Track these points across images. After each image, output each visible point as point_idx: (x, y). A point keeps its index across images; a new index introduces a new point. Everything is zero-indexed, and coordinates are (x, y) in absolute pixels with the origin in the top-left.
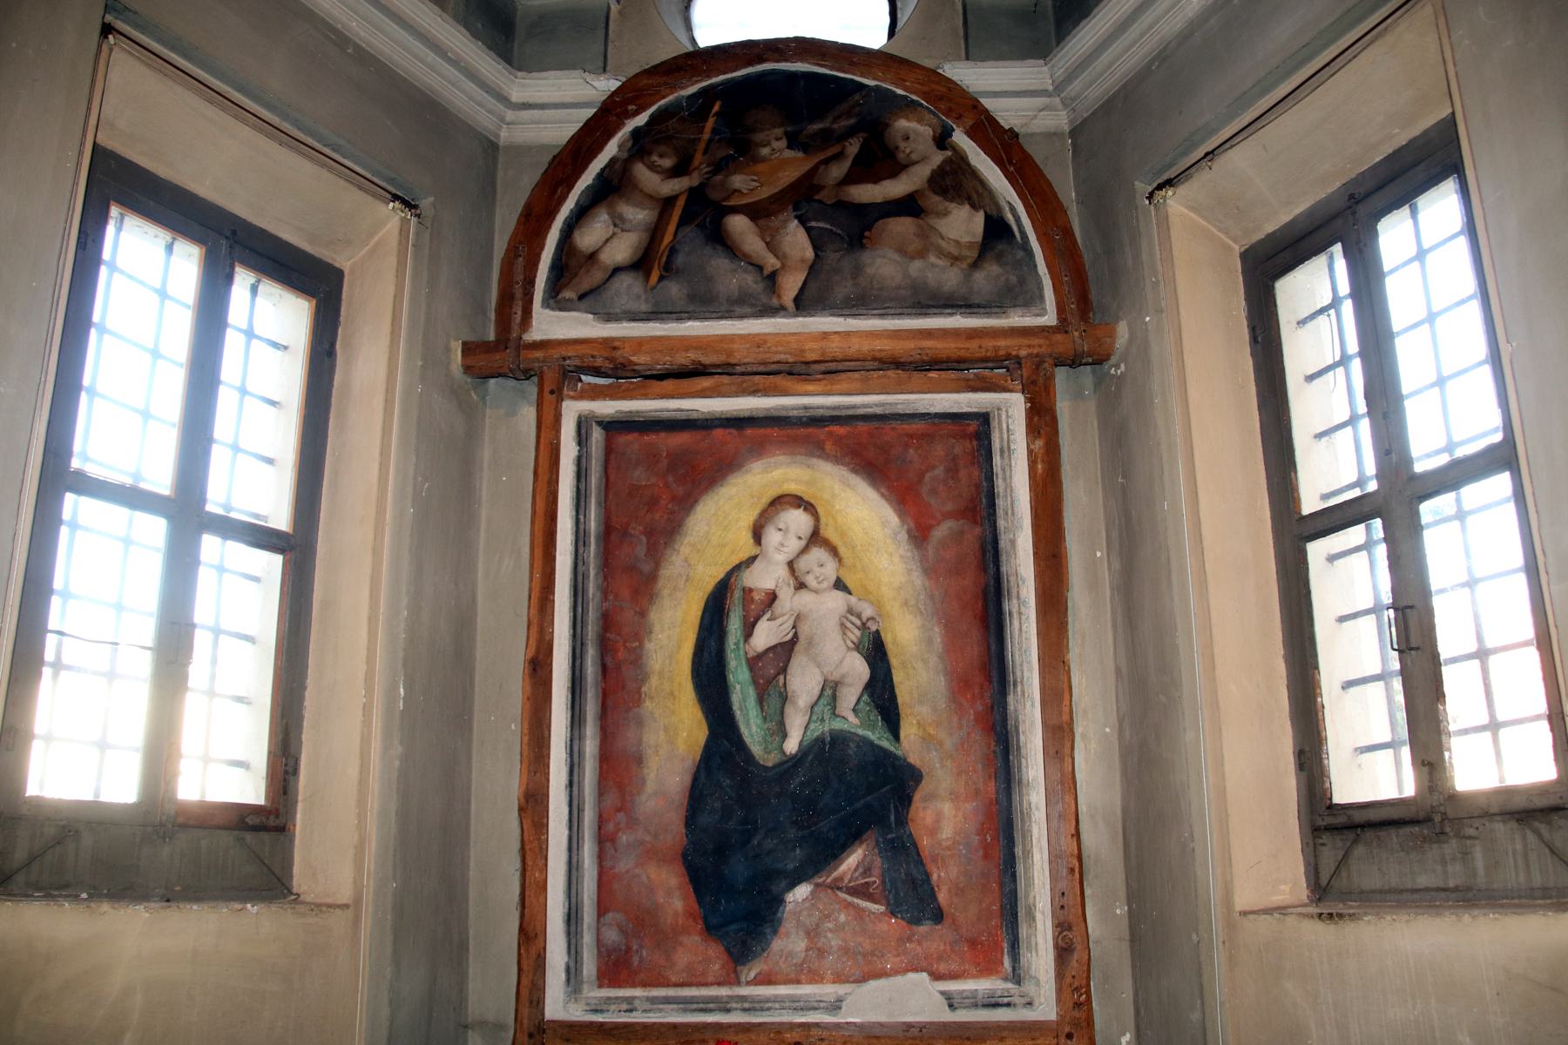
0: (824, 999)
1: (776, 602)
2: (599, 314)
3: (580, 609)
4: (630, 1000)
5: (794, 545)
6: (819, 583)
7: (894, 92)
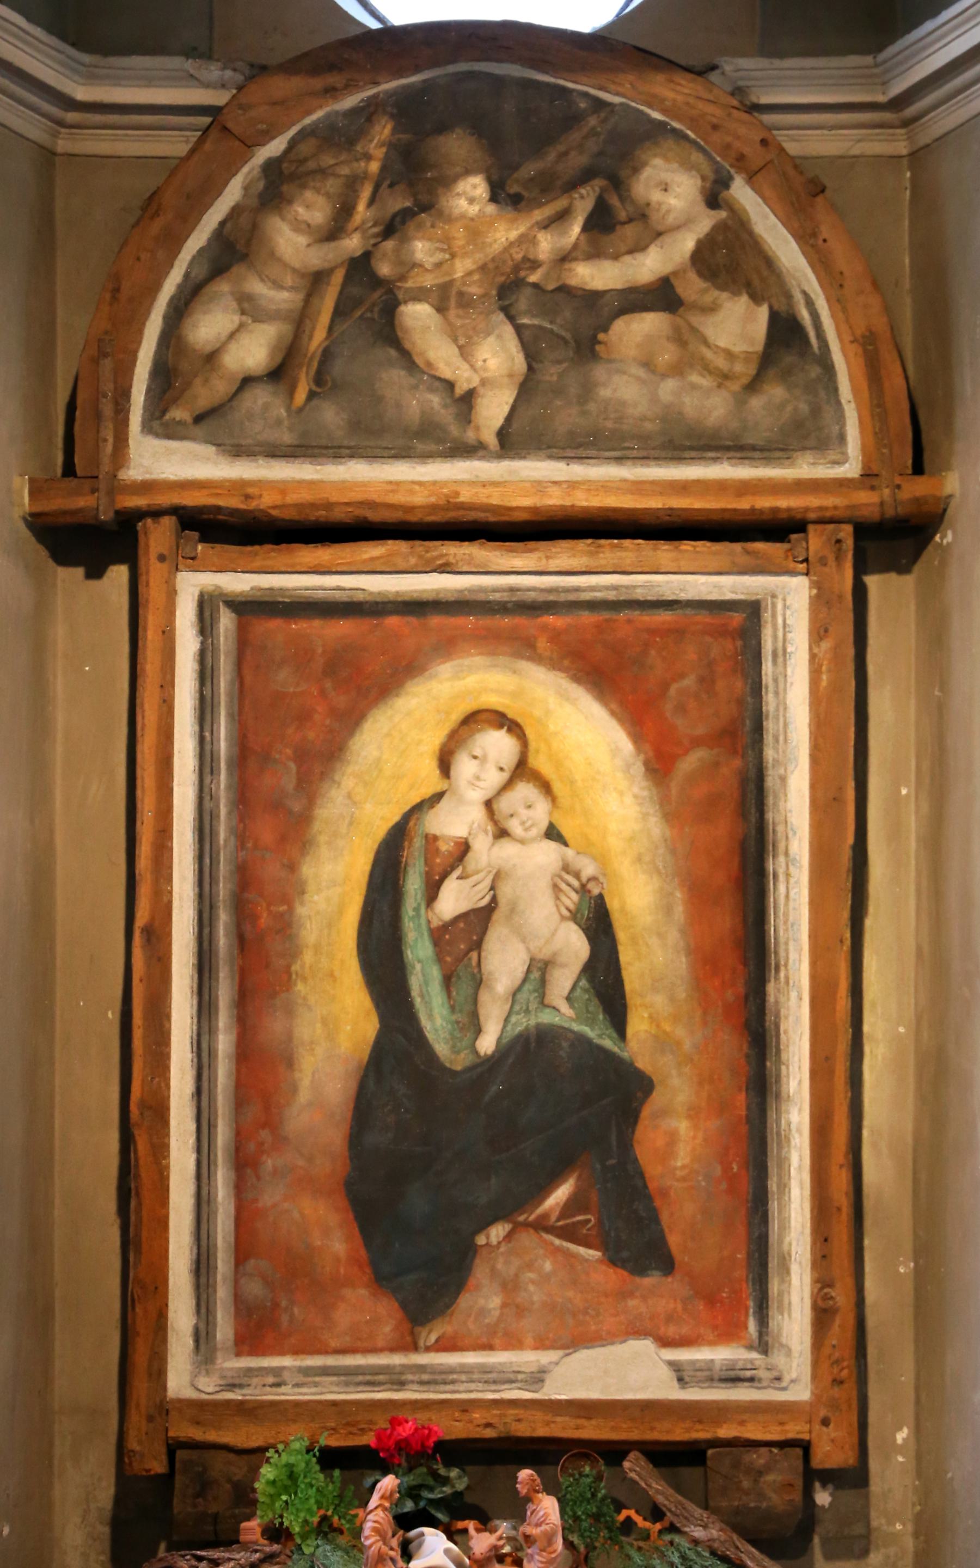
0: (523, 1369)
1: (470, 855)
2: (224, 445)
3: (207, 861)
4: (277, 1371)
5: (494, 779)
6: (526, 830)
7: (647, 116)
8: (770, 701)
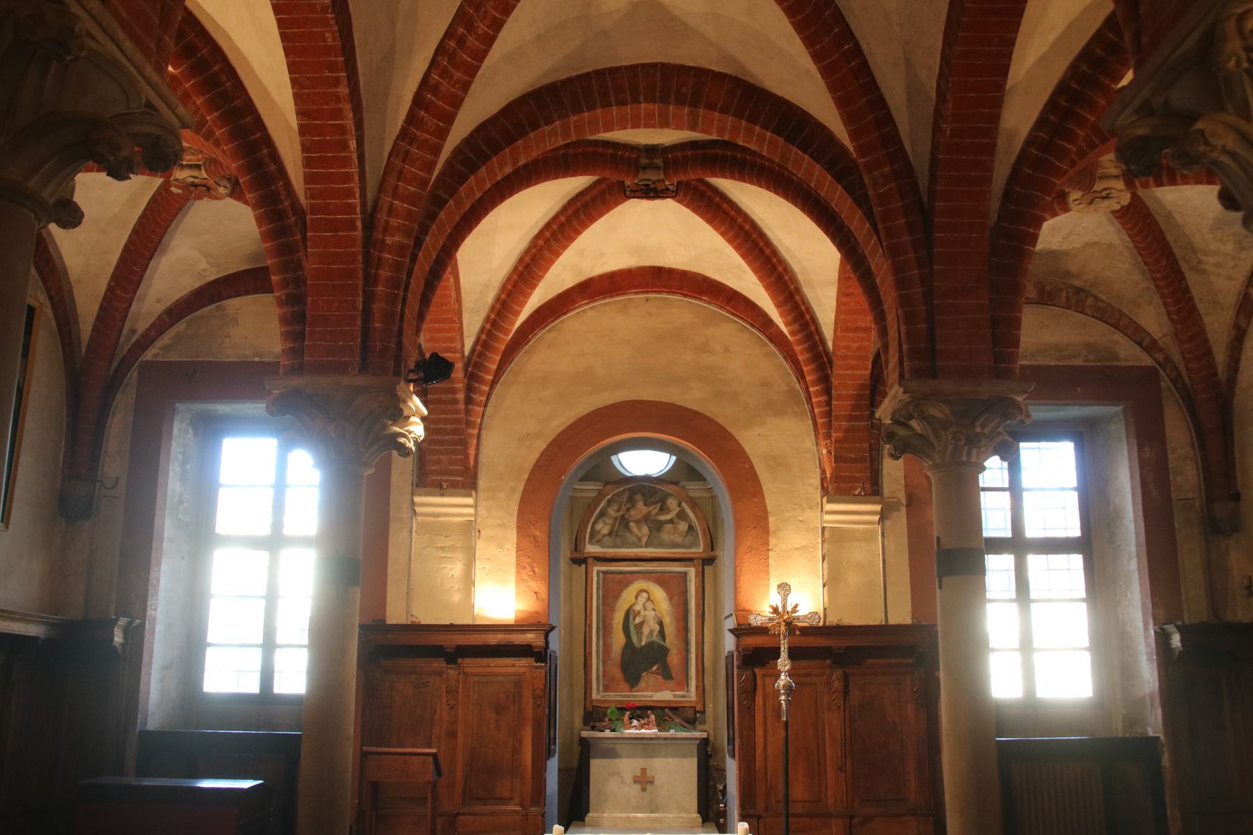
5: (644, 600)
8: (688, 588)
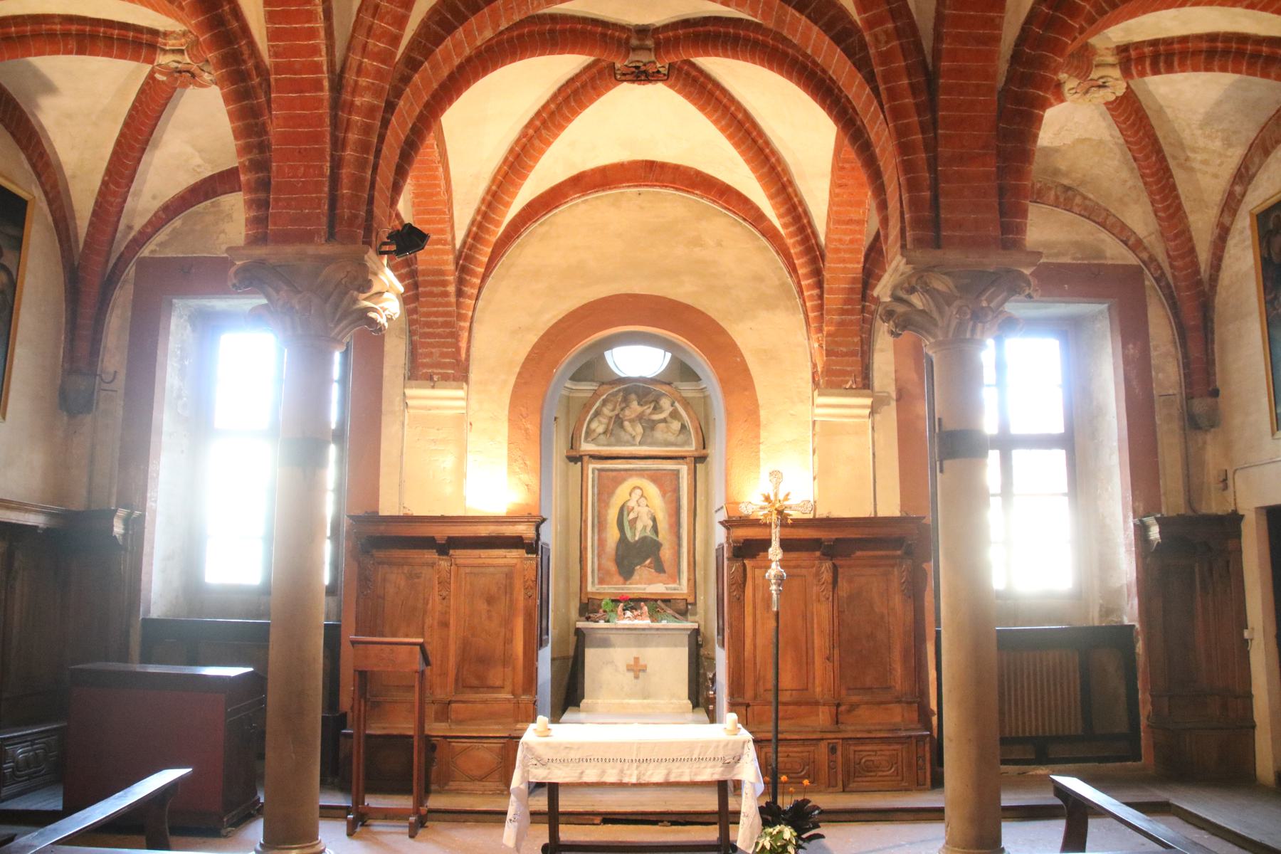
5: (638, 497)
